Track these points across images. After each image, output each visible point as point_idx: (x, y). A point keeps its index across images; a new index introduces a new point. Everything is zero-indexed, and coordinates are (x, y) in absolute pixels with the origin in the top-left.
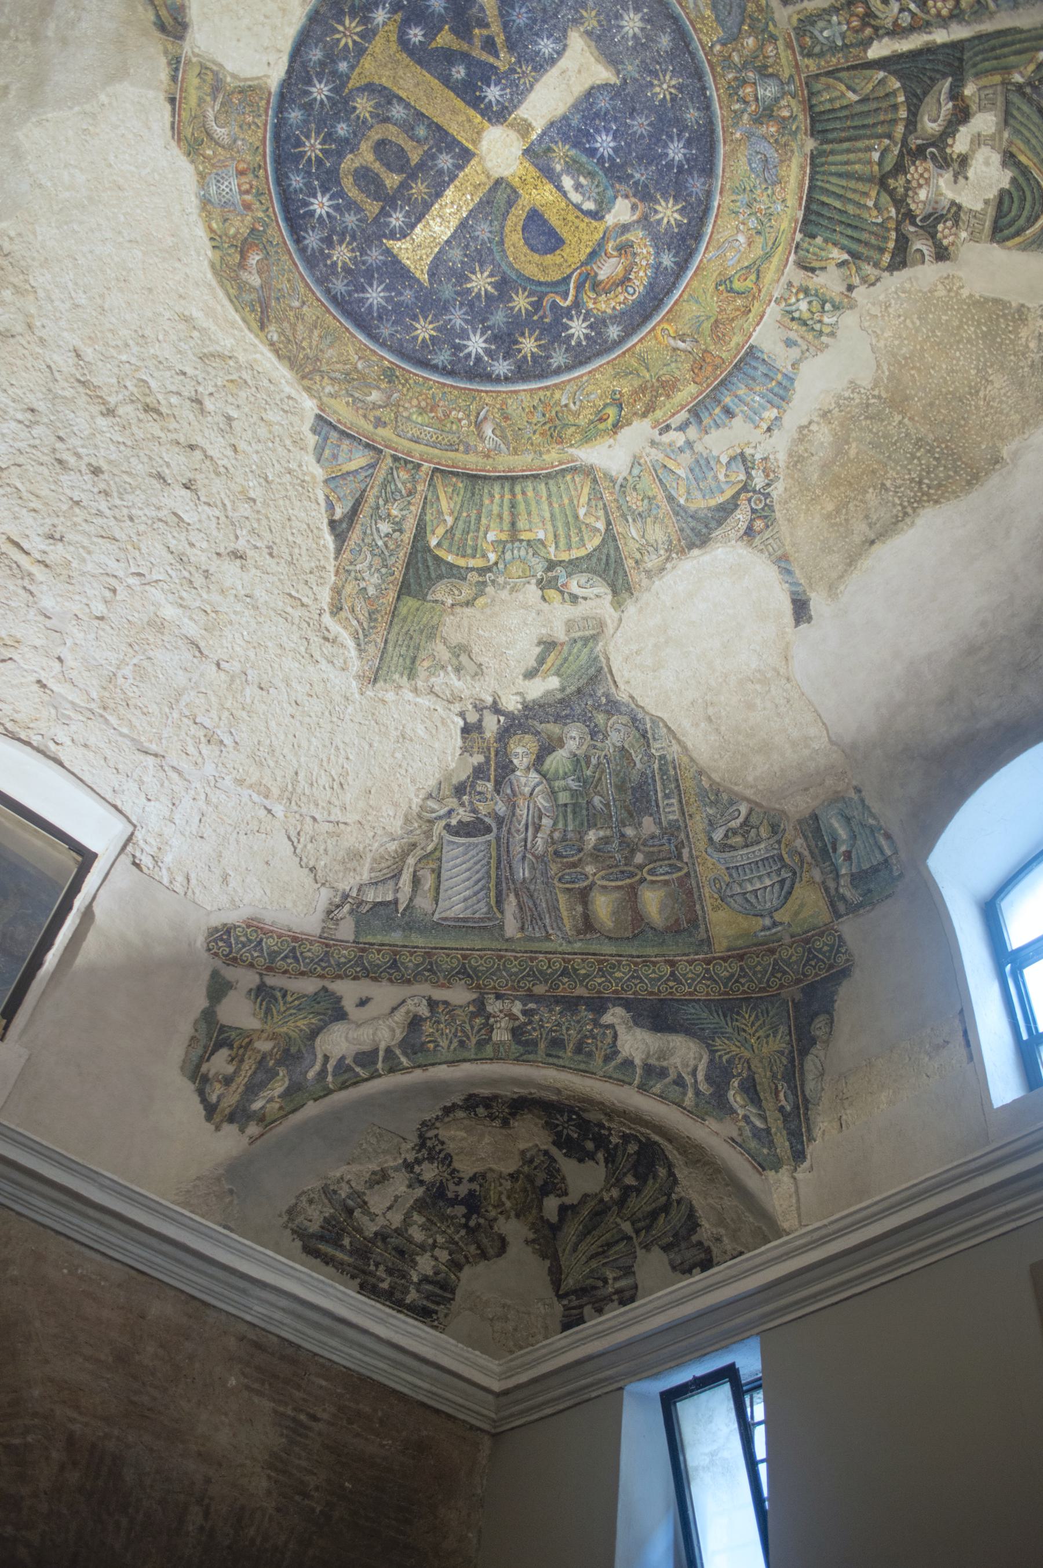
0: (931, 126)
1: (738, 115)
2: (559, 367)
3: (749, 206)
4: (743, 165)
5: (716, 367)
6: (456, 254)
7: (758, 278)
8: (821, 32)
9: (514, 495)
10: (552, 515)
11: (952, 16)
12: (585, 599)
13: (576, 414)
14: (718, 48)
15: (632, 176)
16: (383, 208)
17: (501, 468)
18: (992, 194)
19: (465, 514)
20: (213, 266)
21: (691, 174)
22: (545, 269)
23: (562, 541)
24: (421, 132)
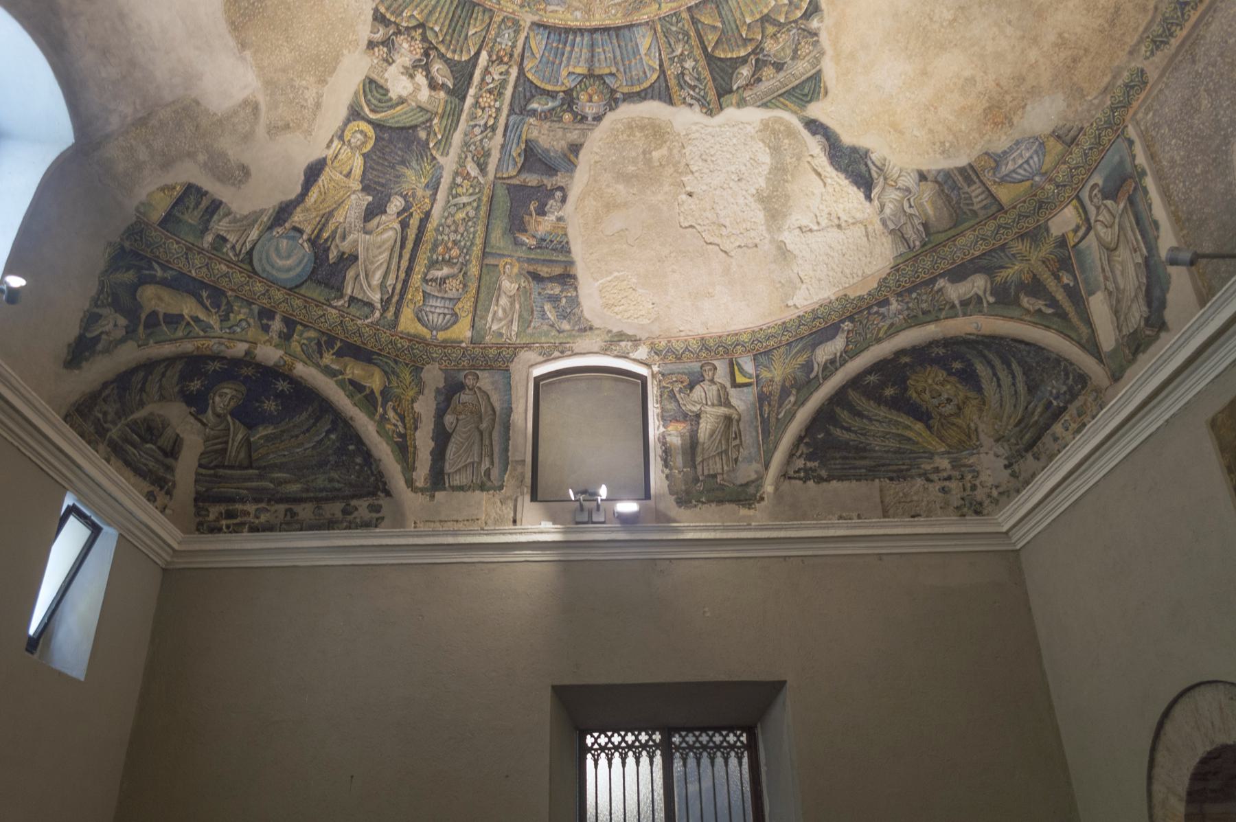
0: (437, 67)
11: (477, 102)
18: (389, 85)
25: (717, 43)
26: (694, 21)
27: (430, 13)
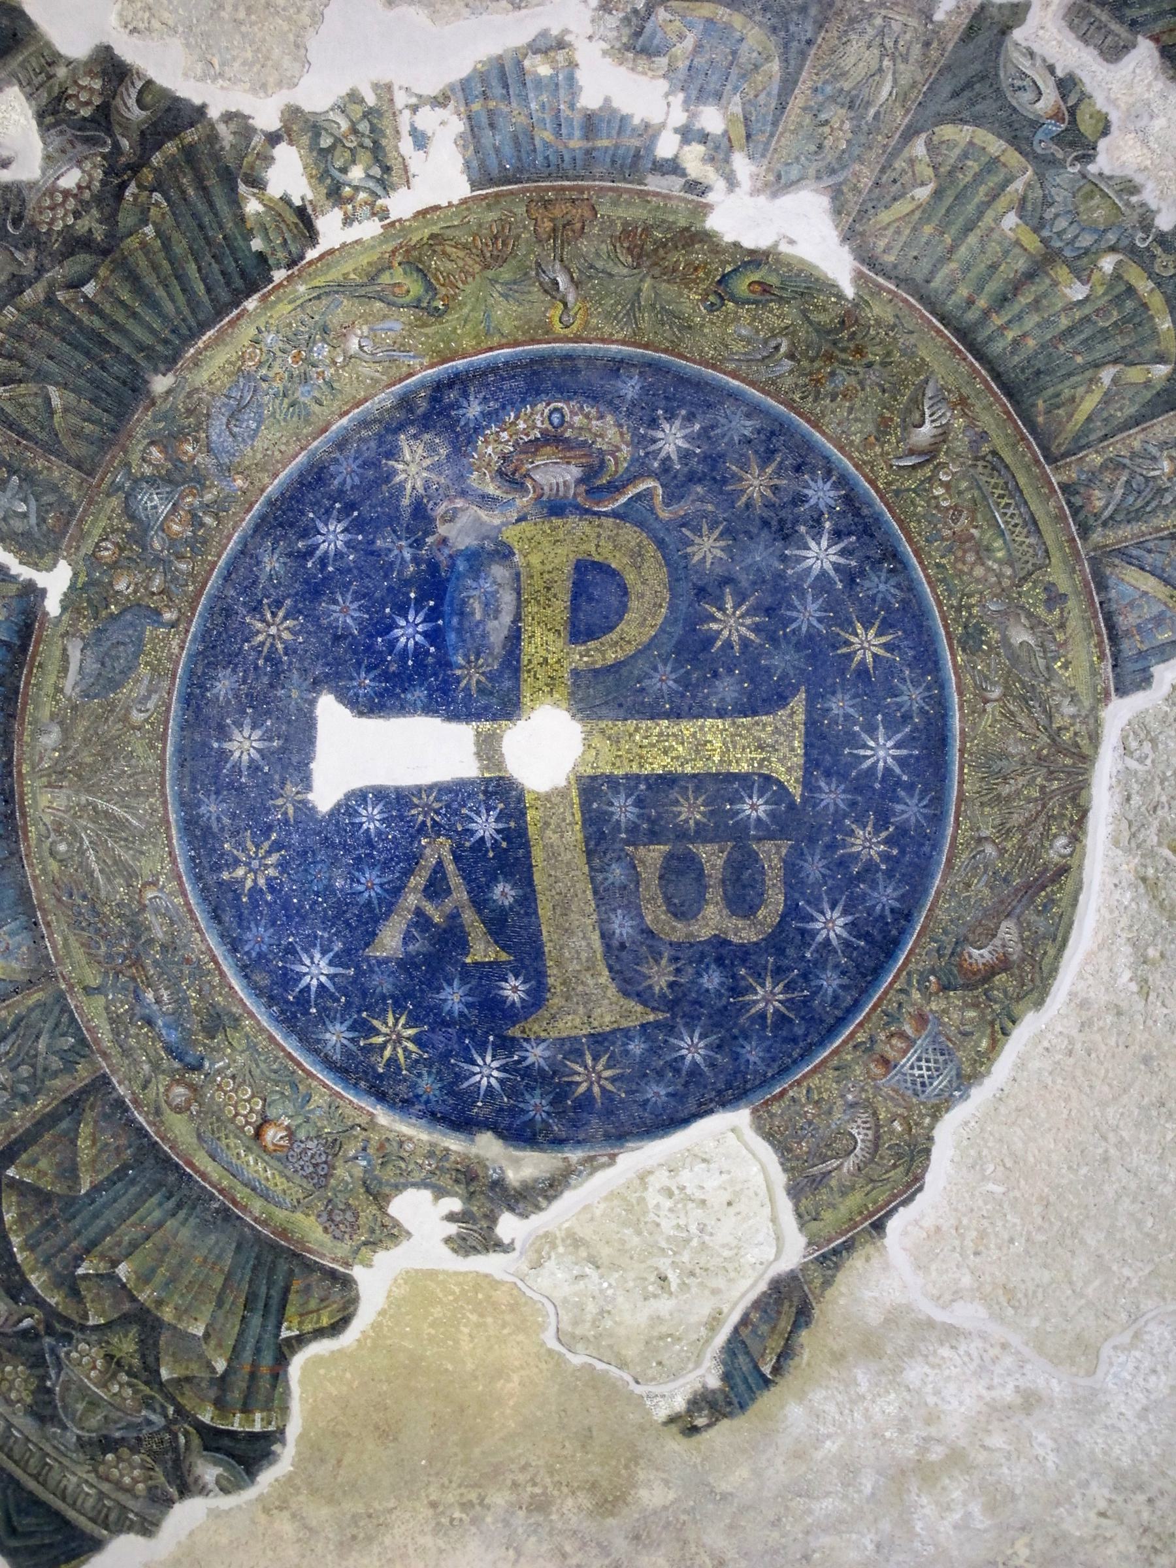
1: (217, 508)
2: (748, 416)
3: (305, 379)
4: (268, 436)
5: (547, 204)
6: (727, 689)
7: (380, 271)
8: (25, 515)
9: (986, 314)
10: (968, 229)
12: (1051, 69)
13: (786, 331)
14: (168, 616)
15: (416, 560)
16: (759, 839)
17: (964, 369)
19: (1079, 359)
20: (1039, 1003)
21: (341, 492)
22: (637, 555)
23: (992, 181)
24: (617, 873)
25: (36, 1191)
26: (73, 1105)
27: (134, 279)
